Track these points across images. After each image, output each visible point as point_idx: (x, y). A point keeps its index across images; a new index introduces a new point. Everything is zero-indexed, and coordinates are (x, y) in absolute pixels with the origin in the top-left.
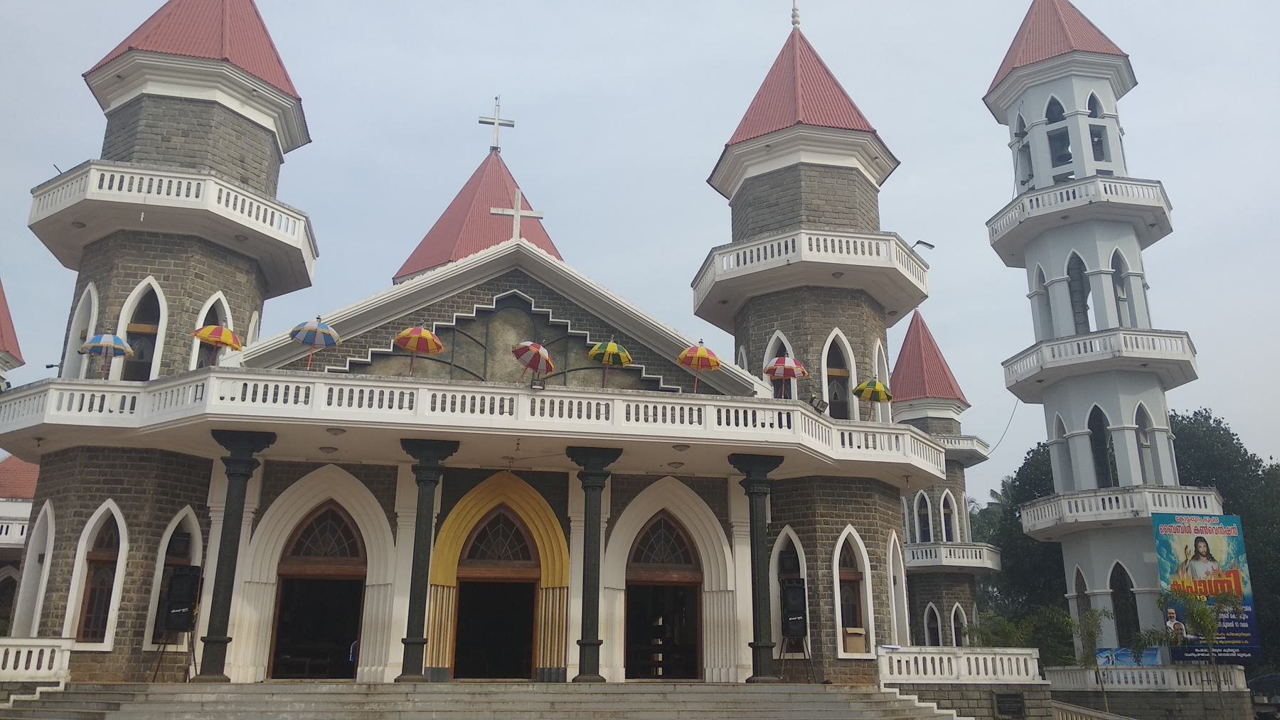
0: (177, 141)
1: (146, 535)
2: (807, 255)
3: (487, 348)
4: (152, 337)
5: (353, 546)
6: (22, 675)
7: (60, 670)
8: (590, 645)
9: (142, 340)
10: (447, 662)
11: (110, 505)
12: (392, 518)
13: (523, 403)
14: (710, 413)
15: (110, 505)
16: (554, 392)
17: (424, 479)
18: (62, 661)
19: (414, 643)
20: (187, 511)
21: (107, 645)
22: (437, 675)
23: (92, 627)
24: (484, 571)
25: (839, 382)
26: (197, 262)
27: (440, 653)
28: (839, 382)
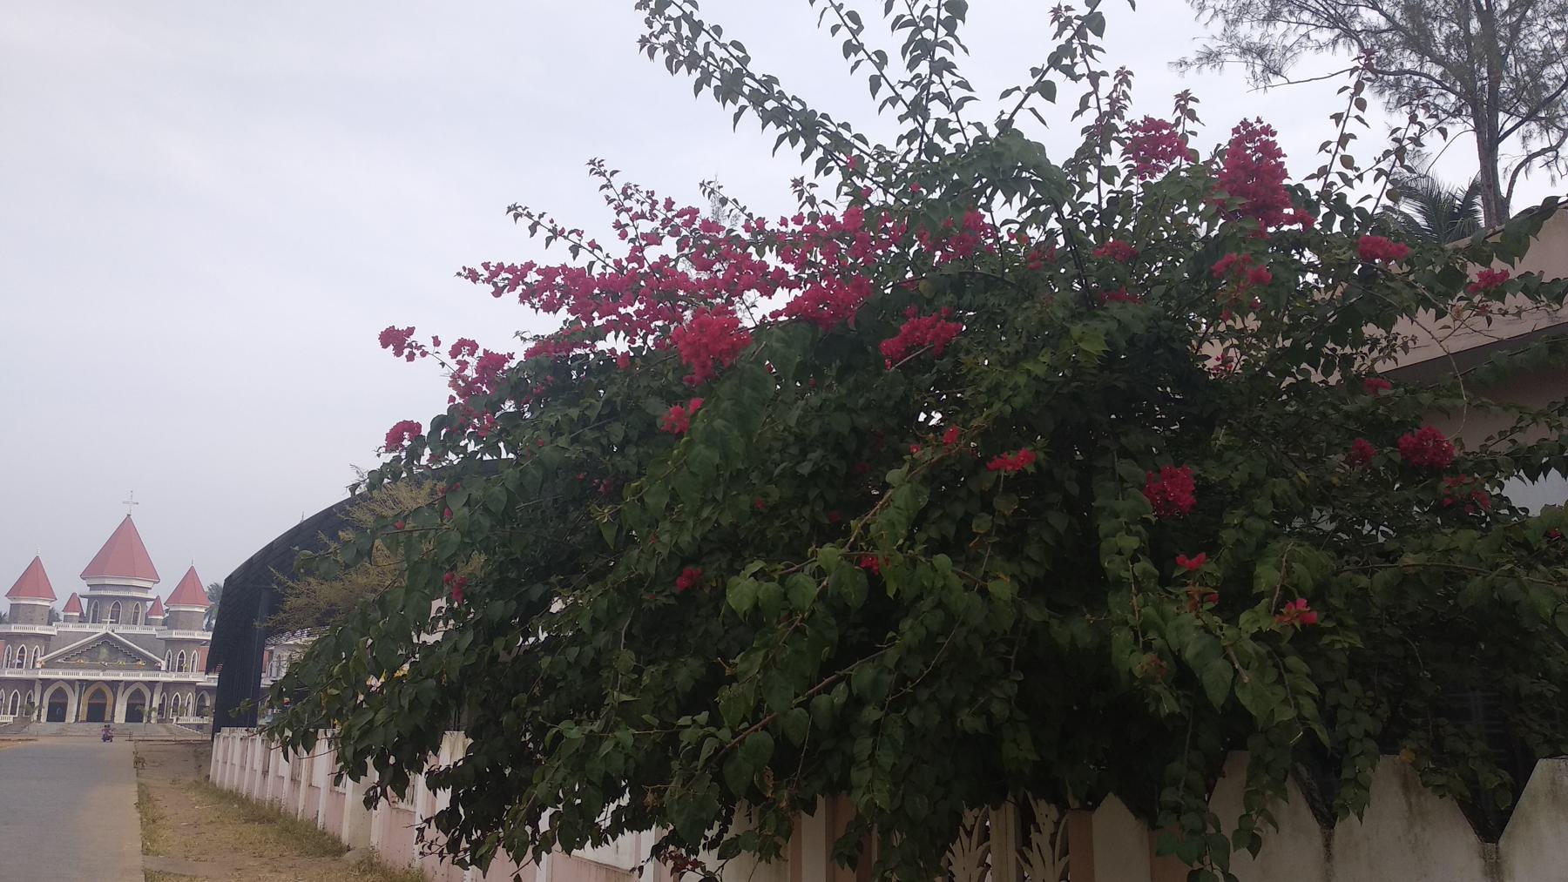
0: (28, 614)
1: (23, 696)
2: (174, 636)
3: (99, 653)
4: (23, 657)
5: (66, 696)
6: (4, 721)
7: (11, 720)
8: (113, 716)
9: (21, 658)
10: (85, 719)
11: (16, 690)
12: (74, 691)
13: (101, 674)
14: (141, 675)
15: (16, 690)
16: (107, 672)
17: (81, 686)
18: (11, 719)
19: (77, 716)
20: (30, 691)
21: (17, 716)
22: (81, 721)
23: (13, 713)
24: (92, 702)
25: (181, 662)
26: (33, 640)
27: (83, 717)
28: (181, 662)
